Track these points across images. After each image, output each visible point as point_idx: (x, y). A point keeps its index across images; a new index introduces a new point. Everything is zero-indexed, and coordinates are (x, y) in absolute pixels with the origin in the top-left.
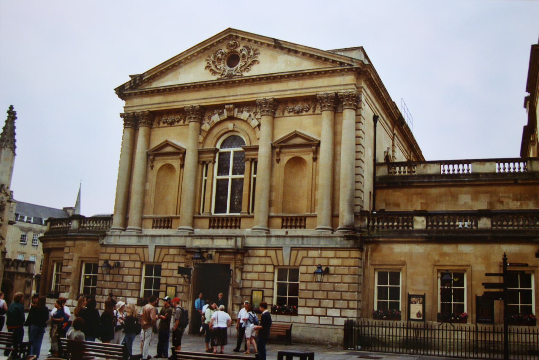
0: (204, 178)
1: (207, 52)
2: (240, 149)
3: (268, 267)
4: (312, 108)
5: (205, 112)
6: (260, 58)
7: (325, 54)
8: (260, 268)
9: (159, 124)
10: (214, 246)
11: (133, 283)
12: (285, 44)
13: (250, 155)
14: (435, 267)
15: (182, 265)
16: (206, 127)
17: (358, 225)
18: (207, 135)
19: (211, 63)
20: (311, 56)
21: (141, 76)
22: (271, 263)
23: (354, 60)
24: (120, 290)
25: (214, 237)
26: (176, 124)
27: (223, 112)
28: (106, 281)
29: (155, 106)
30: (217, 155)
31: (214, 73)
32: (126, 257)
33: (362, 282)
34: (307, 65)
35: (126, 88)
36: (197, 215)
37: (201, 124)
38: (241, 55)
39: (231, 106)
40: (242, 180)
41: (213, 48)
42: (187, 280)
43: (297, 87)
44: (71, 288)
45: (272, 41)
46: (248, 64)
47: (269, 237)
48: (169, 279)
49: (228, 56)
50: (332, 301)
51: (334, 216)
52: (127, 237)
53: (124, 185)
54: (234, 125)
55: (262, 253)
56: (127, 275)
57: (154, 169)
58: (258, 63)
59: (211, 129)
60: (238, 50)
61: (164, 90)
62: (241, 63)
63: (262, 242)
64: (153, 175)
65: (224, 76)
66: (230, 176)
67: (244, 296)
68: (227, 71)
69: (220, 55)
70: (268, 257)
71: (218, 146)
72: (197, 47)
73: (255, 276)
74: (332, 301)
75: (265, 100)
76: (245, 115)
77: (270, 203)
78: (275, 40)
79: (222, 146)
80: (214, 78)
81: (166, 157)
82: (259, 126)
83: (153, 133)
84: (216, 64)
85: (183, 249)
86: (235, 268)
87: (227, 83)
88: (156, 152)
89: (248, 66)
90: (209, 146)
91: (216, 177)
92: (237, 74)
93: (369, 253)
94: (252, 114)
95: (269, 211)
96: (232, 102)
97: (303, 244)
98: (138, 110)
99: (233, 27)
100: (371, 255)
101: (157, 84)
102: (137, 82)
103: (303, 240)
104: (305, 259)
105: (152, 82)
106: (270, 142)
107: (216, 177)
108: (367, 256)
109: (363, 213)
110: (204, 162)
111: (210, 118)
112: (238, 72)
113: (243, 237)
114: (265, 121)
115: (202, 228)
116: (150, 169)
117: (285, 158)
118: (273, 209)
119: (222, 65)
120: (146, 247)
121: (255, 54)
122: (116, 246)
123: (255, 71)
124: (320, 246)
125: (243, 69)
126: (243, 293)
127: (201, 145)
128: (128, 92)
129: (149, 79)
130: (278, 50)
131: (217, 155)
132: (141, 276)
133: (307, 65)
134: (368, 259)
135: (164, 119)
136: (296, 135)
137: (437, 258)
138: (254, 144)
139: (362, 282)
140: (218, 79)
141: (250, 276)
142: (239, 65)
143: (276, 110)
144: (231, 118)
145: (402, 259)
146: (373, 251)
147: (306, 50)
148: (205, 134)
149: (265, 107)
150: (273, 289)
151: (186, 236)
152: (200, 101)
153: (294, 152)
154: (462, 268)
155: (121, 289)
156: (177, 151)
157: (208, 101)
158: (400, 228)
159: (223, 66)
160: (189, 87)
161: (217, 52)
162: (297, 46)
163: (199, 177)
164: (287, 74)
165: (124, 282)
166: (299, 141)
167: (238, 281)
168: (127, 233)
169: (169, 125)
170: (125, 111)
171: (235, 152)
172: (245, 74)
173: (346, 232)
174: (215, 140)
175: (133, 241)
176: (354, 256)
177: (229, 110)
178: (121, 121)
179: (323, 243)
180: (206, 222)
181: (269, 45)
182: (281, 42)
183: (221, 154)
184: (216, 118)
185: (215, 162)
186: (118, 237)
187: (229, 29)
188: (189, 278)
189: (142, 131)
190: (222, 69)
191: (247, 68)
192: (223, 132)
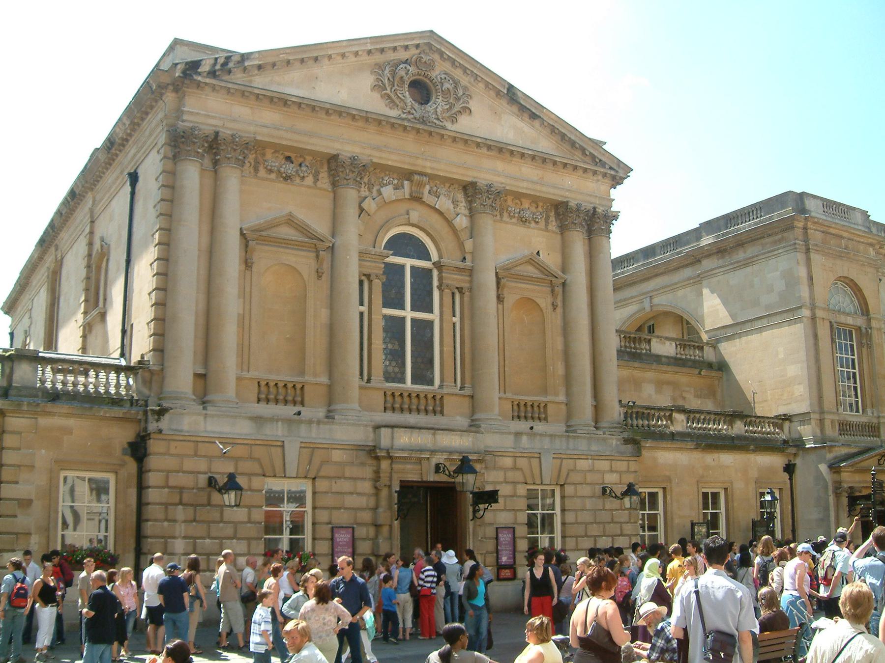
4: (543, 219)
11: (249, 525)
20: (563, 136)
35: (199, 70)
48: (335, 513)
50: (610, 539)
65: (412, 116)
70: (518, 469)
74: (610, 539)
84: (396, 87)
97: (568, 449)
101: (260, 81)
112: (438, 119)
123: (465, 125)
165: (225, 522)
182: (519, 94)
187: (431, 32)
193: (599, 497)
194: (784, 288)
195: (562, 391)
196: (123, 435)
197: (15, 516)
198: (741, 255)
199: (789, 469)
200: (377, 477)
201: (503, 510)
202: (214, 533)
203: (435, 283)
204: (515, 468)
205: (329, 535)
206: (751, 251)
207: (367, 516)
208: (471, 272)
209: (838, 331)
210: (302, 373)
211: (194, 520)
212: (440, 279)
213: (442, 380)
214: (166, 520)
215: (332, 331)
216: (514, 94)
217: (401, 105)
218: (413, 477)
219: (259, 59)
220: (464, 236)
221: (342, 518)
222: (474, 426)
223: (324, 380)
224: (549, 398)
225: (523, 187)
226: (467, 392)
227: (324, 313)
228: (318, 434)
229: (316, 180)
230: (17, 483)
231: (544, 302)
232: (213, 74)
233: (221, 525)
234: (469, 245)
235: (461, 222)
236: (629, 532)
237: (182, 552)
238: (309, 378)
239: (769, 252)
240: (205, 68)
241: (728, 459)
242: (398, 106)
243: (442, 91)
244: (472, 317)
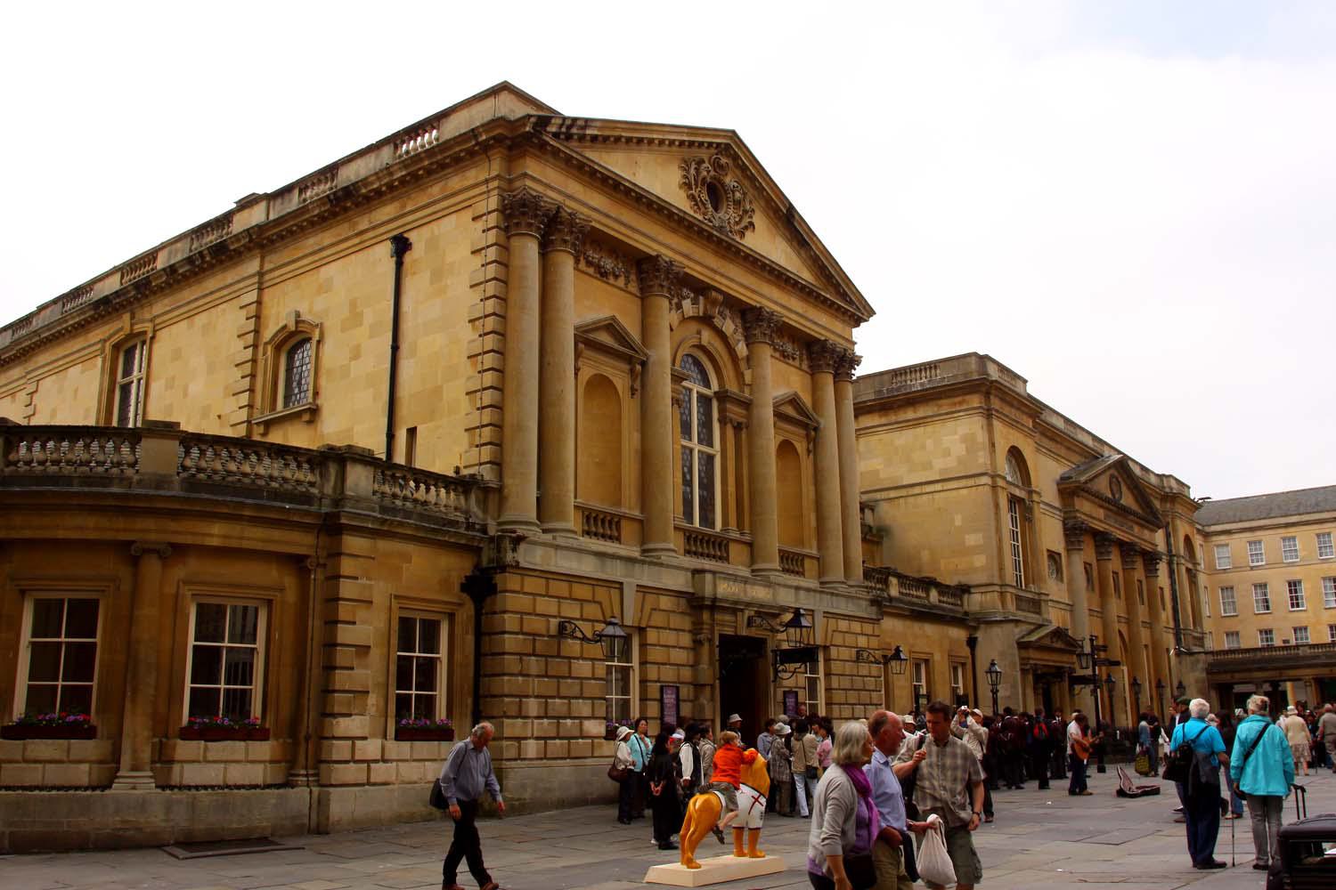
12: (800, 224)
24: (566, 701)
34: (806, 275)
39: (720, 298)
43: (800, 311)
45: (785, 206)
52: (573, 555)
56: (577, 658)
61: (628, 191)
72: (686, 130)
78: (791, 208)
81: (602, 358)
96: (724, 289)
99: (738, 132)
112: (731, 232)
122: (548, 575)
133: (806, 275)
144: (706, 320)
147: (822, 253)
155: (569, 698)
160: (671, 215)
162: (815, 239)
169: (598, 276)
181: (777, 210)
193: (854, 662)
194: (964, 453)
195: (814, 543)
196: (456, 567)
198: (910, 414)
199: (972, 642)
200: (696, 631)
202: (564, 692)
203: (715, 415)
205: (658, 696)
206: (922, 411)
207: (686, 674)
208: (747, 405)
209: (1014, 501)
210: (618, 503)
211: (546, 676)
212: (722, 411)
213: (725, 522)
215: (646, 458)
216: (793, 217)
217: (703, 209)
218: (729, 631)
219: (600, 128)
220: (743, 365)
221: (668, 674)
222: (758, 576)
223: (636, 513)
224: (806, 551)
225: (793, 320)
226: (747, 538)
227: (636, 436)
228: (647, 577)
229: (627, 282)
231: (800, 446)
232: (556, 135)
234: (748, 378)
235: (742, 349)
236: (875, 702)
237: (535, 714)
238: (624, 510)
239: (947, 414)
241: (930, 629)
243: (734, 201)
244: (751, 456)
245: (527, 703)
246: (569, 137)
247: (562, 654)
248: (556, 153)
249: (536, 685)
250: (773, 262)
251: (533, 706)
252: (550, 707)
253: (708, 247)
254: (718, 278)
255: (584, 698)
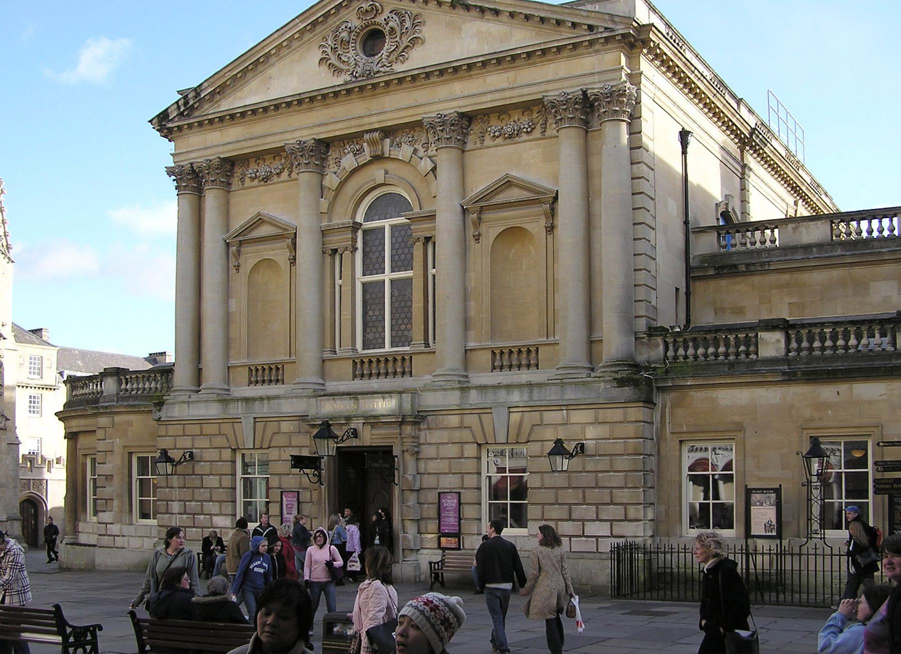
0: (338, 282)
1: (319, 29)
2: (401, 220)
3: (466, 447)
5: (328, 152)
6: (426, 31)
7: (556, 13)
8: (453, 451)
9: (242, 180)
10: (360, 412)
13: (421, 230)
14: (805, 432)
15: (305, 453)
16: (332, 181)
17: (642, 358)
18: (336, 197)
19: (329, 50)
21: (197, 90)
22: (471, 439)
23: (617, 19)
25: (359, 396)
26: (275, 179)
27: (361, 151)
28: (173, 488)
29: (230, 147)
30: (360, 234)
31: (337, 71)
32: (203, 442)
33: (655, 469)
36: (328, 355)
37: (322, 176)
38: (388, 28)
40: (409, 280)
41: (331, 20)
42: (315, 479)
44: (116, 503)
46: (403, 46)
47: (464, 389)
49: (362, 34)
51: (592, 343)
53: (190, 303)
54: (386, 172)
55: (454, 420)
57: (242, 270)
58: (423, 43)
59: (342, 184)
60: (380, 19)
62: (388, 46)
63: (453, 399)
64: (240, 282)
66: (387, 276)
67: (424, 504)
68: (361, 64)
69: (344, 35)
71: (359, 218)
73: (443, 465)
75: (440, 116)
76: (405, 151)
77: (466, 324)
79: (368, 217)
80: (339, 80)
81: (261, 247)
82: (434, 170)
83: (233, 201)
85: (304, 421)
86: (403, 452)
87: (362, 88)
88: (241, 238)
89: (403, 51)
90: (341, 218)
91: (360, 279)
92: (381, 69)
93: (667, 410)
94: (418, 146)
95: (465, 338)
96: (376, 126)
98: (199, 158)
100: (672, 414)
102: (191, 102)
103: (531, 393)
104: (536, 429)
105: (220, 100)
106: (457, 202)
107: (361, 279)
108: (663, 416)
109: (653, 331)
110: (335, 251)
111: (338, 163)
113: (414, 392)
114: (446, 160)
115: (340, 379)
116: (233, 271)
117: (490, 232)
118: (472, 333)
119: (352, 53)
120: (235, 421)
121: (414, 26)
124: (564, 403)
125: (392, 57)
126: (422, 500)
127: (326, 217)
128: (176, 124)
129: (212, 94)
130: (460, 11)
131: (360, 234)
132: (234, 475)
134: (665, 423)
135: (250, 171)
136: (508, 183)
137: (808, 413)
138: (427, 208)
139: (655, 469)
140: (346, 83)
141: (432, 466)
142: (384, 52)
143: (465, 135)
145: (736, 419)
146: (676, 405)
148: (330, 195)
149: (442, 131)
150: (479, 489)
151: (309, 397)
152: (316, 130)
153: (505, 219)
154: (864, 431)
156: (280, 231)
157: (330, 127)
158: (732, 358)
159: (354, 55)
161: (338, 27)
163: (328, 281)
164: (480, 59)
166: (514, 194)
167: (410, 478)
168: (202, 396)
170: (174, 163)
171: (393, 227)
172: (399, 67)
173: (616, 372)
174: (352, 205)
175: (214, 410)
176: (633, 419)
177: (372, 143)
178: (170, 183)
179: (571, 395)
180: (348, 367)
183: (366, 232)
184: (349, 162)
185: (355, 249)
186: (185, 406)
188: (320, 476)
189: (212, 199)
190: (352, 61)
191: (401, 54)
192: (366, 188)
197: (105, 487)
201: (448, 473)
204: (461, 427)
214: (167, 487)
225: (487, 102)
230: (104, 463)
233: (202, 490)
240: (173, 114)
242: (342, 70)
245: (172, 505)
246: (192, 109)
247: (196, 473)
248: (190, 126)
249: (176, 494)
250: (424, 68)
251: (176, 507)
252: (204, 508)
253: (352, 99)
254: (366, 120)
255: (214, 501)
